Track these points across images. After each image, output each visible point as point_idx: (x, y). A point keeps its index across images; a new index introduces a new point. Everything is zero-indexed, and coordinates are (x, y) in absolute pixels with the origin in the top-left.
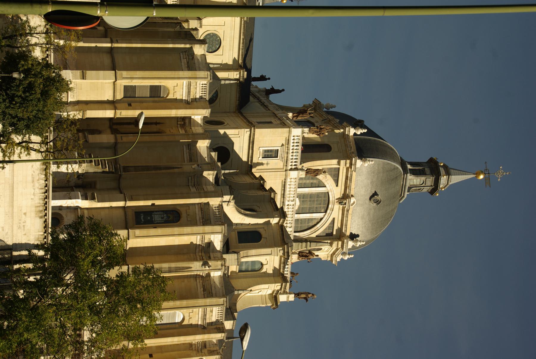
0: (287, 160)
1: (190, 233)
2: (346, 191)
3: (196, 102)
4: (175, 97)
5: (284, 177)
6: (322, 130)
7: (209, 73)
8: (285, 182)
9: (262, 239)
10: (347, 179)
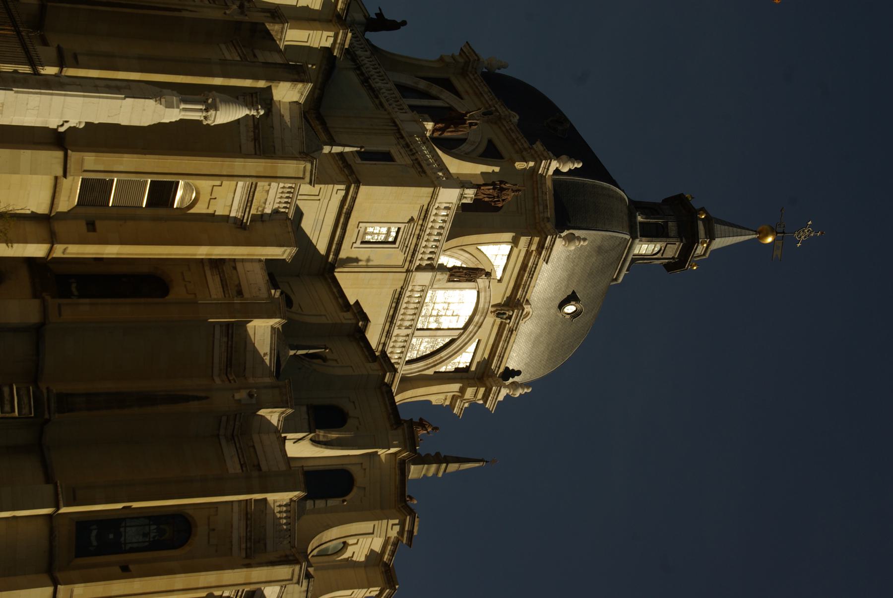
0: (415, 250)
1: (213, 584)
2: (517, 293)
3: (263, 221)
4: (210, 211)
5: (401, 283)
6: (504, 192)
7: (309, 166)
8: (400, 294)
9: (355, 490)
10: (525, 271)
